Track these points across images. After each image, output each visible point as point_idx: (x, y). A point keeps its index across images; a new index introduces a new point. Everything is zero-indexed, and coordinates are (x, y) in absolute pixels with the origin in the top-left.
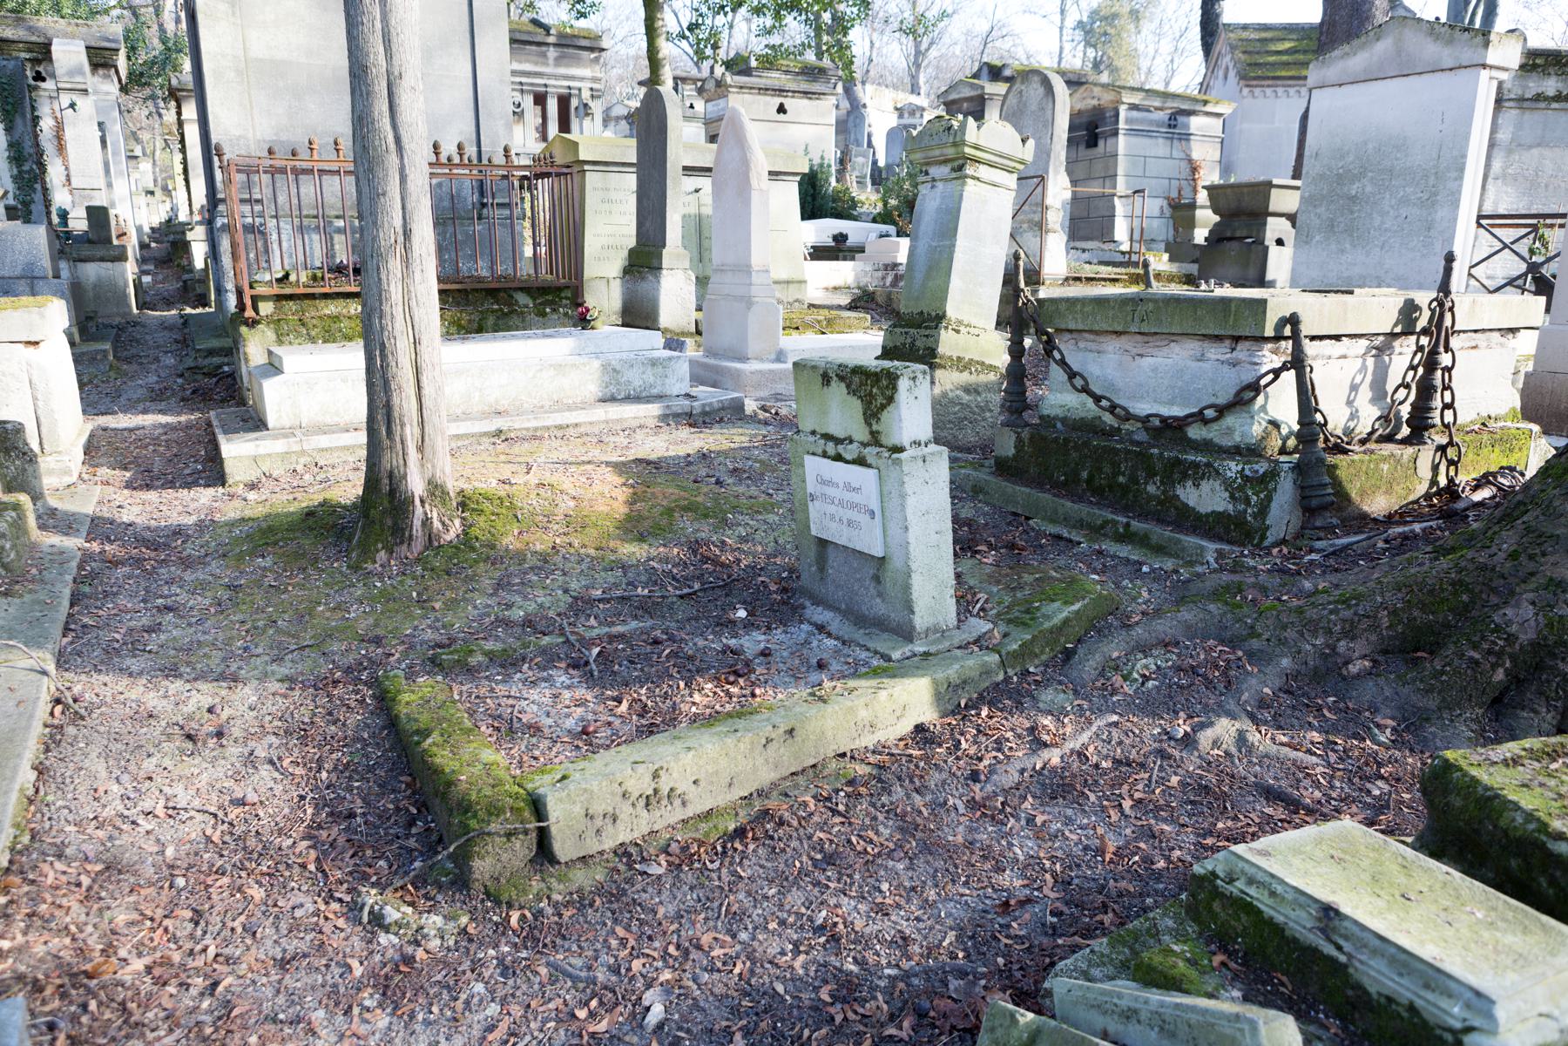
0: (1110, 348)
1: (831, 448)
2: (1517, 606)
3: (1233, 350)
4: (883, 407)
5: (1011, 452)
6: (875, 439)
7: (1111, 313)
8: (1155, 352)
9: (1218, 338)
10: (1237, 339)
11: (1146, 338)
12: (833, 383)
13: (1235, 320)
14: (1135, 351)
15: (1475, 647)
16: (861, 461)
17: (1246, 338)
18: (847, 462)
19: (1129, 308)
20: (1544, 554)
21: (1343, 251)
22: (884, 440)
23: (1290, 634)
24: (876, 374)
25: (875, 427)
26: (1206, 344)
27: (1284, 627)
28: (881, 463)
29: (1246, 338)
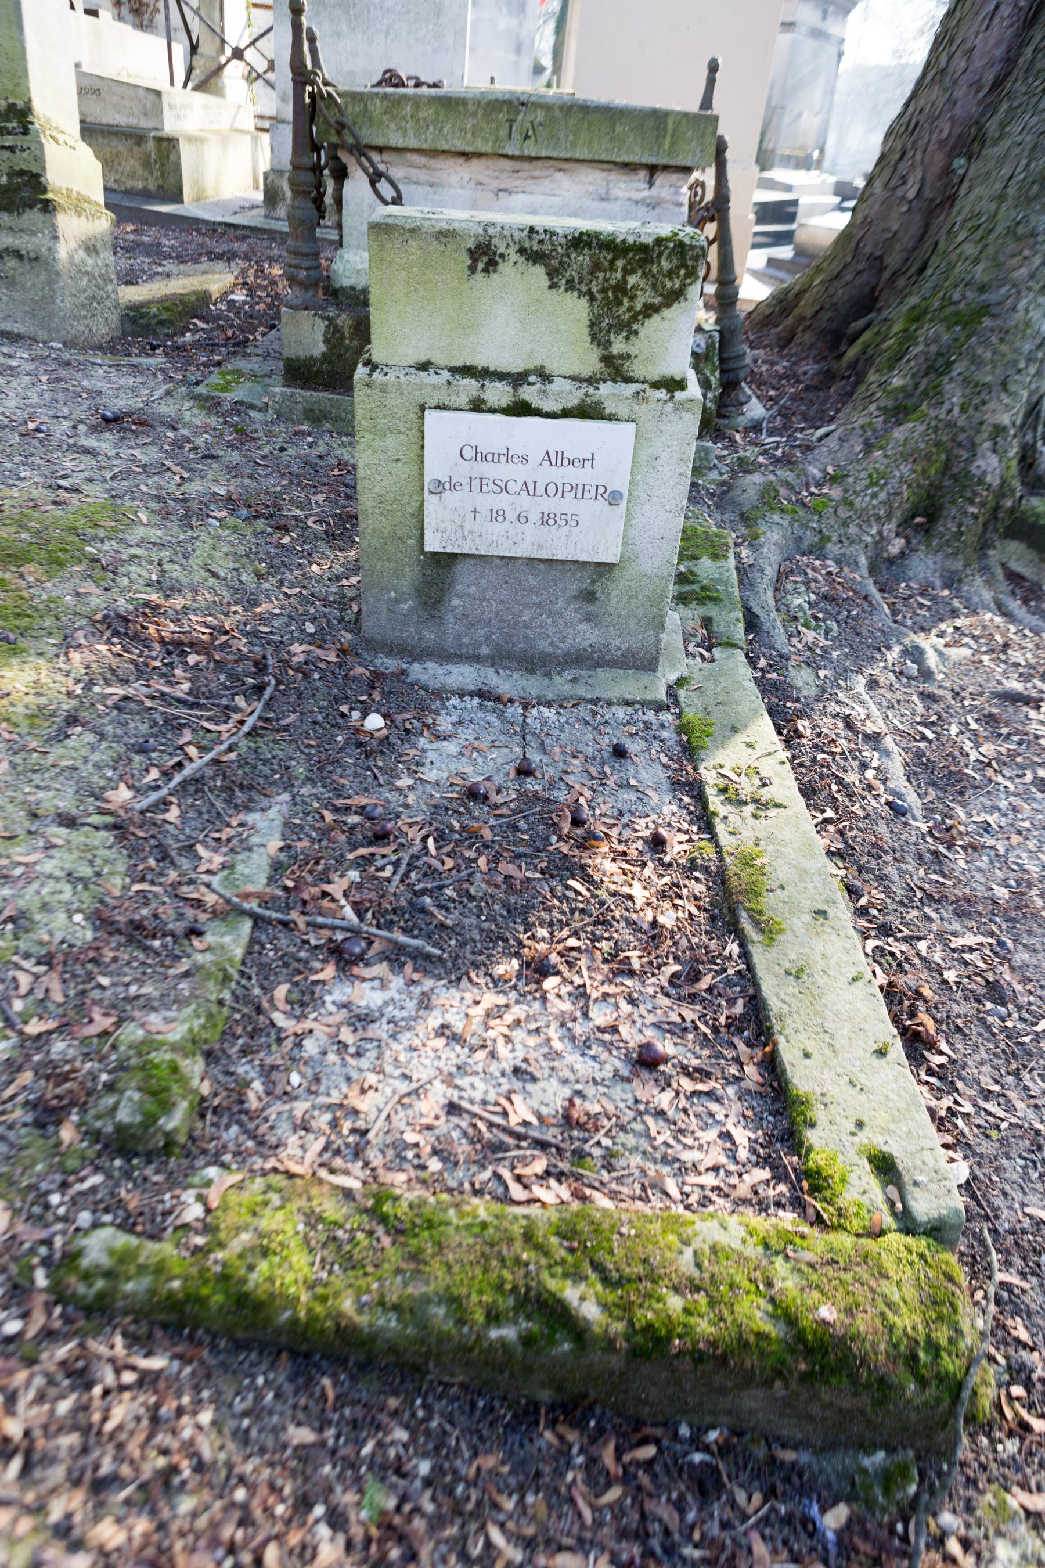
0: (454, 179)
1: (498, 393)
2: (983, 457)
3: (651, 184)
4: (650, 310)
5: (319, 348)
6: (615, 369)
7: (469, 124)
8: (529, 185)
9: (628, 167)
10: (653, 170)
11: (518, 165)
12: (505, 268)
13: (673, 143)
14: (496, 184)
15: (972, 503)
16: (587, 412)
17: (666, 168)
18: (492, 411)
19: (502, 116)
20: (984, 403)
21: (339, 34)
22: (637, 369)
23: (853, 530)
24: (643, 248)
25: (618, 346)
26: (613, 176)
27: (845, 524)
28: (641, 410)
29: (666, 168)
